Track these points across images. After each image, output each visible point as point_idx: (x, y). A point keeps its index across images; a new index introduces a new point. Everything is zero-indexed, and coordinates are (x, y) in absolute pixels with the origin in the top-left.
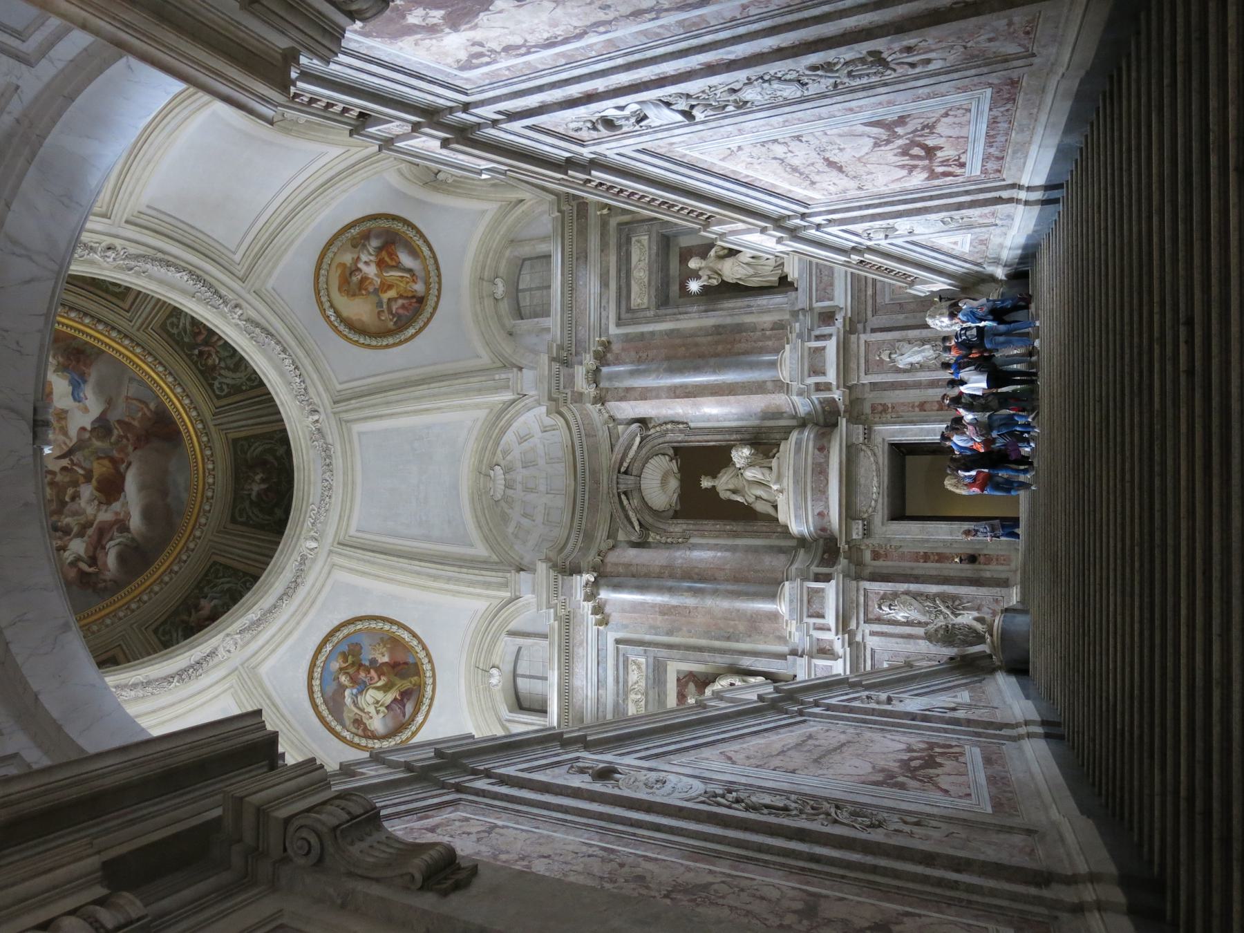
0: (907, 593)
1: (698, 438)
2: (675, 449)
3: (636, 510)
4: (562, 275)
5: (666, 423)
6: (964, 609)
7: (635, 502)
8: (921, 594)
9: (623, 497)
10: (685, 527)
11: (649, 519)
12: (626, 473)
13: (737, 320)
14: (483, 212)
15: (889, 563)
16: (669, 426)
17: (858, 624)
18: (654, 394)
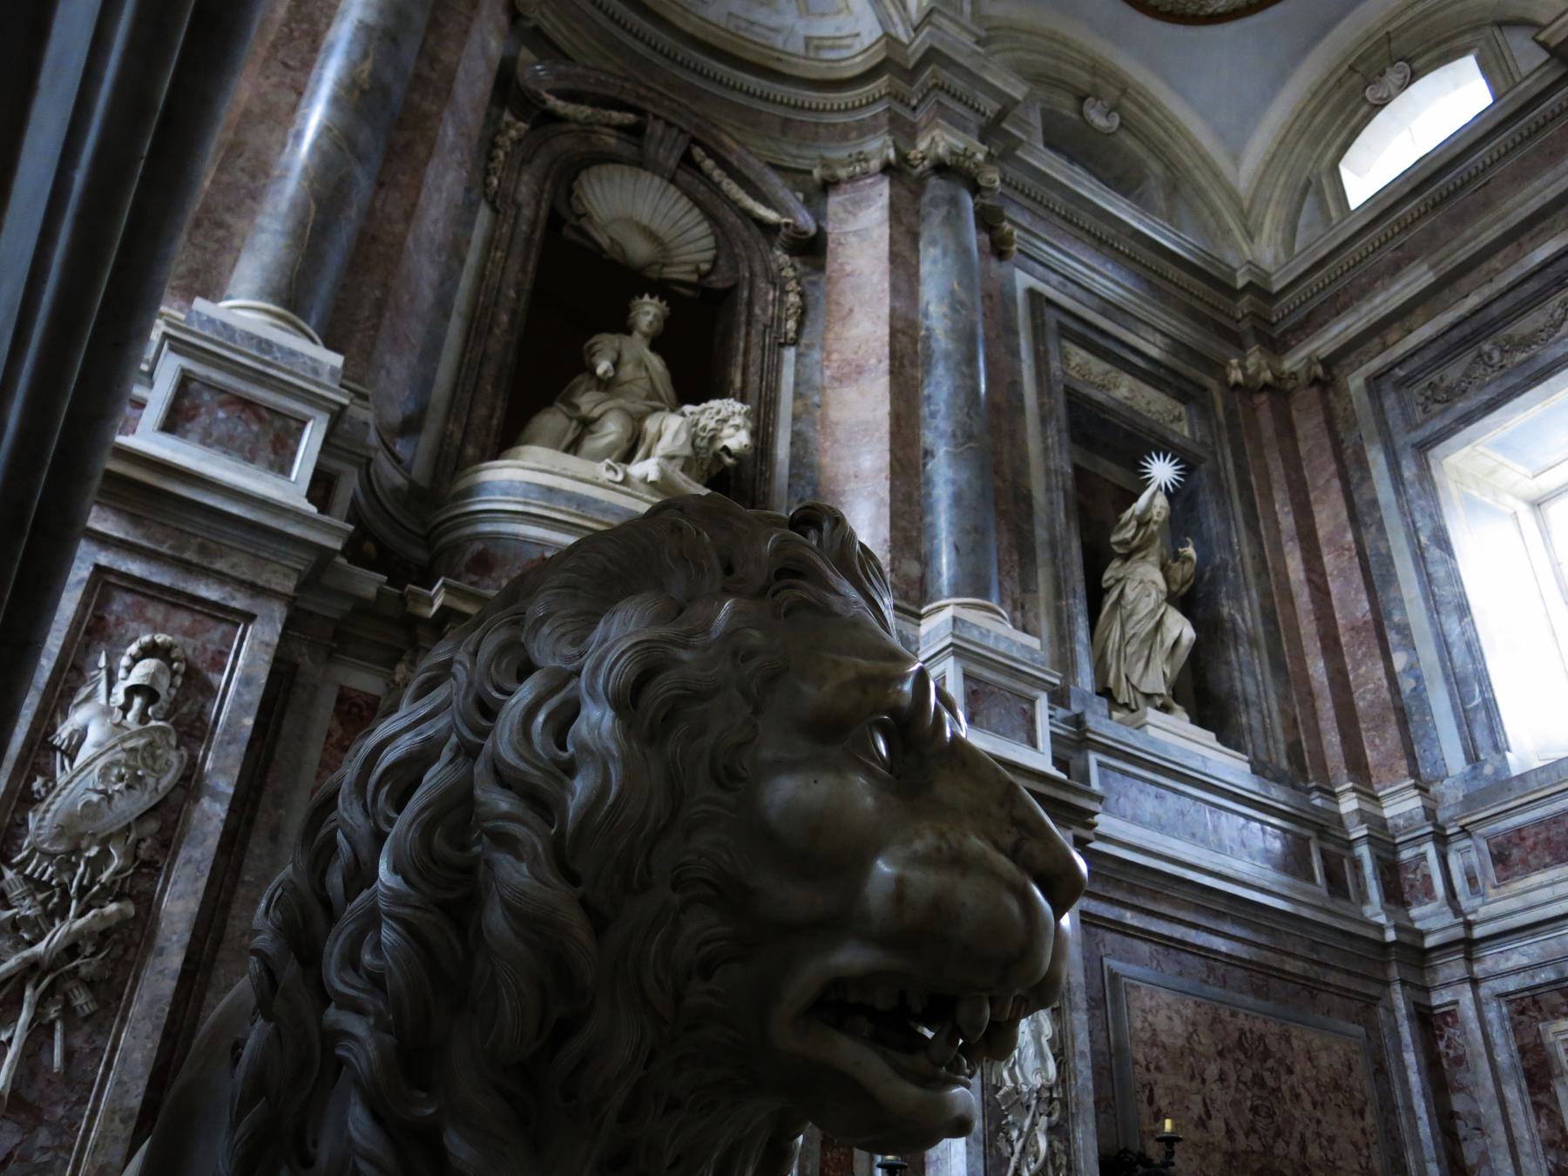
0: (191, 782)
1: (755, 354)
2: (730, 293)
3: (587, 127)
4: (1137, 234)
5: (802, 295)
6: (40, 1032)
7: (611, 141)
8: (168, 843)
9: (629, 118)
10: (527, 212)
11: (564, 144)
12: (687, 160)
13: (1042, 555)
14: (1236, 158)
15: (314, 753)
16: (793, 298)
17: (103, 541)
18: (904, 286)
